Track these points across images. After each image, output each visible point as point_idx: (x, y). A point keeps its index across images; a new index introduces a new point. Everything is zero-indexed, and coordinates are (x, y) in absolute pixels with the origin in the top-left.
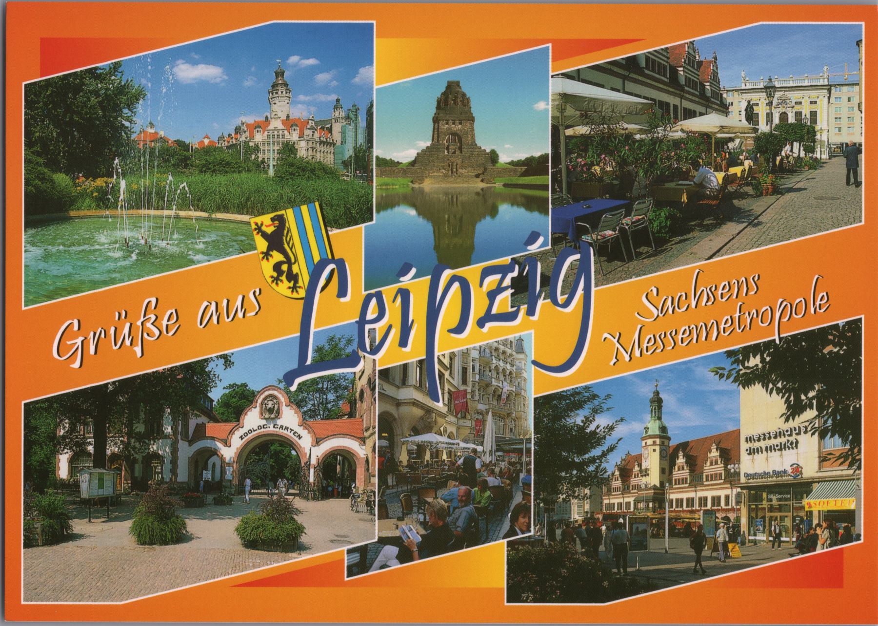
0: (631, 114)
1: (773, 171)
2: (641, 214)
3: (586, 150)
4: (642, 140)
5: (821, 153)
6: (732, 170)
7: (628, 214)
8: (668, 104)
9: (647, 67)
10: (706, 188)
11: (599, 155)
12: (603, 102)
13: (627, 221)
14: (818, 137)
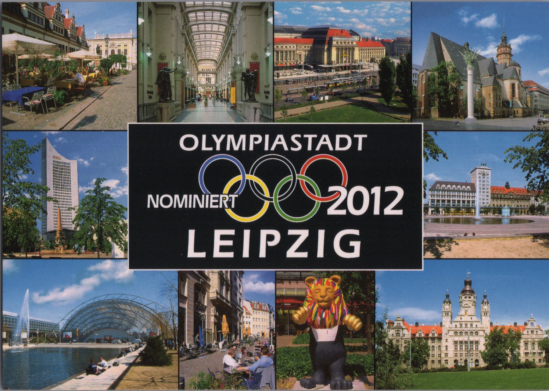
0: (47, 50)
1: (108, 75)
2: (51, 93)
3: (27, 65)
4: (52, 61)
5: (129, 68)
6: (90, 75)
7: (45, 93)
8: (63, 46)
9: (54, 30)
10: (79, 82)
11: (33, 68)
12: (35, 44)
13: (45, 96)
14: (128, 60)
